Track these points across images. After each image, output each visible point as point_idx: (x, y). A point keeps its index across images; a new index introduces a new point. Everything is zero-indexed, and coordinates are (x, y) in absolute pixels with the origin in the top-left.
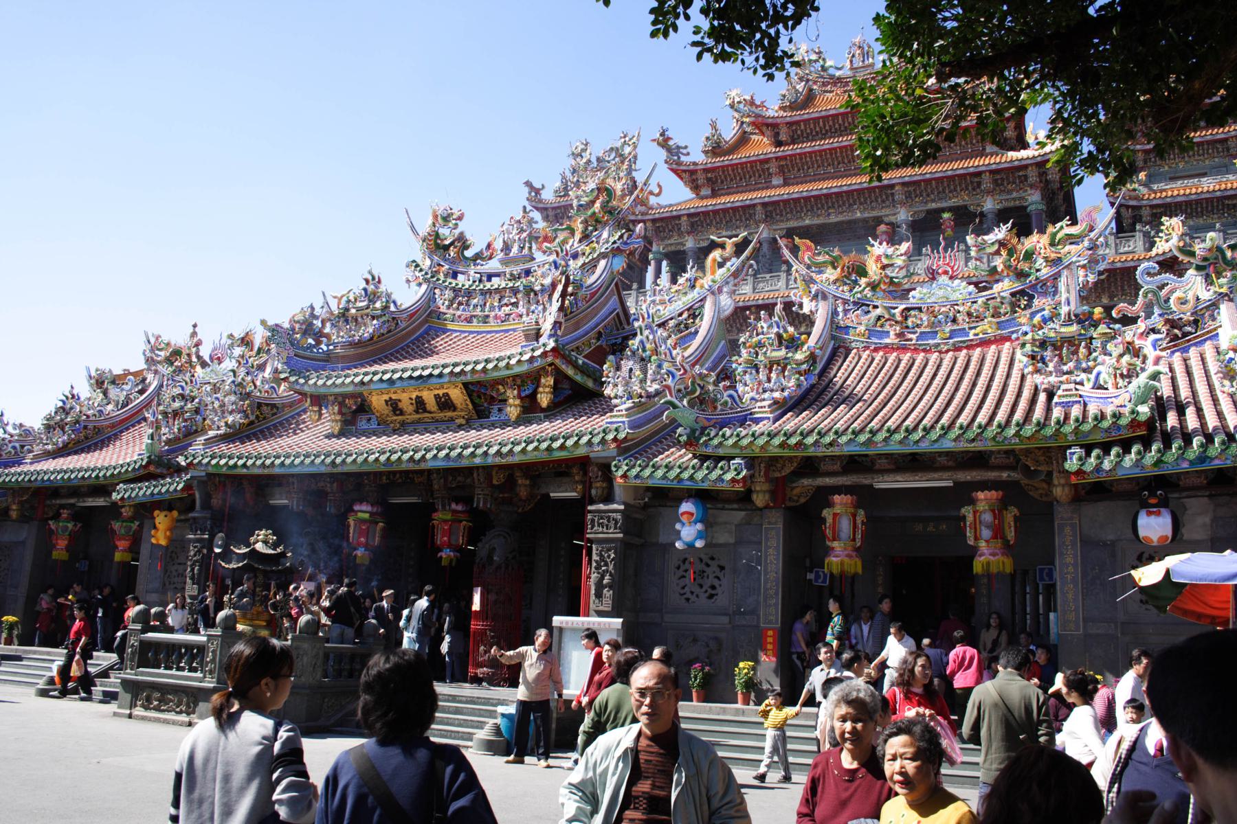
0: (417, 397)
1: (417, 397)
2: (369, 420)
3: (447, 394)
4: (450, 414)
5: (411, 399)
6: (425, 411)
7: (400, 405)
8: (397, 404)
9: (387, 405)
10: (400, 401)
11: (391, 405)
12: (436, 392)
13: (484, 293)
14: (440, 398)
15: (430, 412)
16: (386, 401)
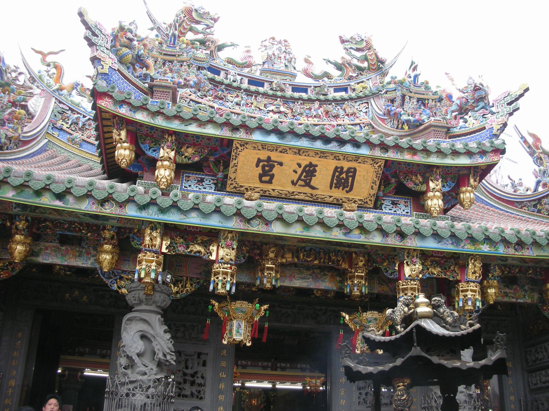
0: (311, 165)
1: (311, 165)
2: (202, 180)
3: (355, 170)
4: (339, 194)
5: (299, 165)
6: (308, 184)
7: (276, 170)
8: (272, 167)
9: (257, 166)
10: (281, 164)
11: (263, 167)
12: (339, 164)
13: (248, 93)
14: (341, 172)
15: (313, 188)
16: (259, 161)
